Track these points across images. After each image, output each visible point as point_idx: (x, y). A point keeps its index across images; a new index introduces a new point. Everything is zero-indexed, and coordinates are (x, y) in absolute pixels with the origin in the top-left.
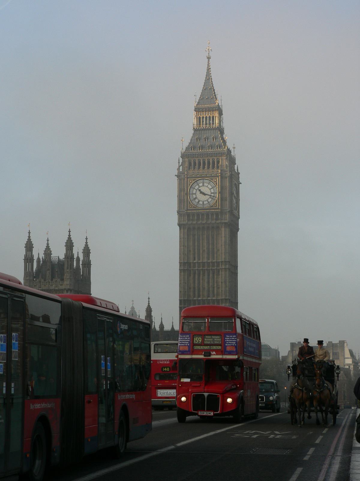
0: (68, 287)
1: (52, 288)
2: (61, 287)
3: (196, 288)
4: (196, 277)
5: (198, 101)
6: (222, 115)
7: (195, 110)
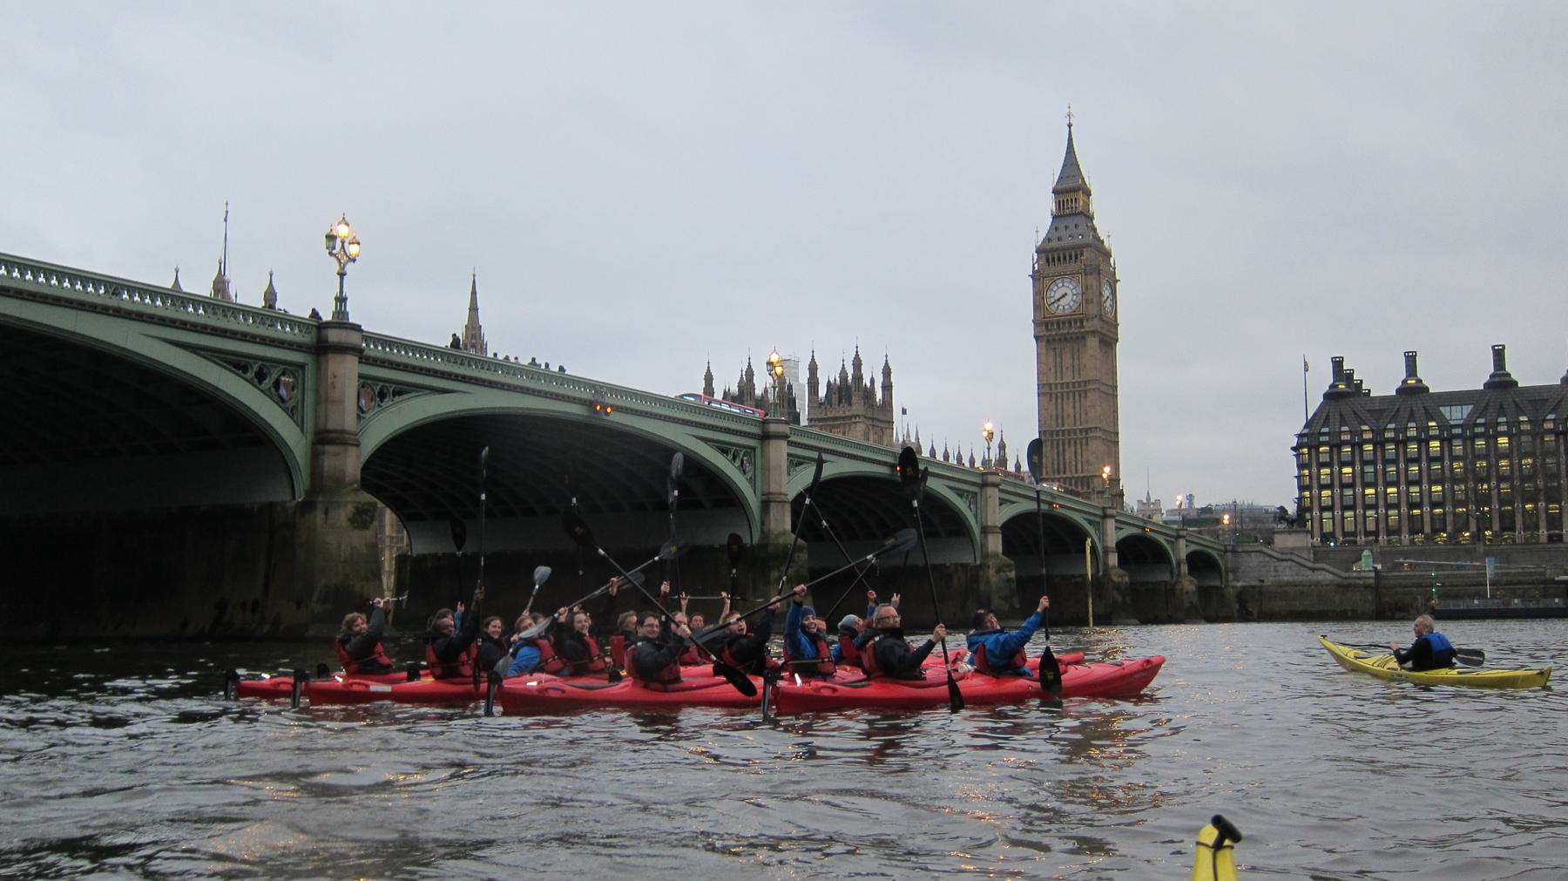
0: (855, 413)
1: (837, 415)
2: (848, 414)
3: (1060, 417)
4: (1059, 401)
5: (1056, 181)
6: (1090, 195)
7: (1053, 192)
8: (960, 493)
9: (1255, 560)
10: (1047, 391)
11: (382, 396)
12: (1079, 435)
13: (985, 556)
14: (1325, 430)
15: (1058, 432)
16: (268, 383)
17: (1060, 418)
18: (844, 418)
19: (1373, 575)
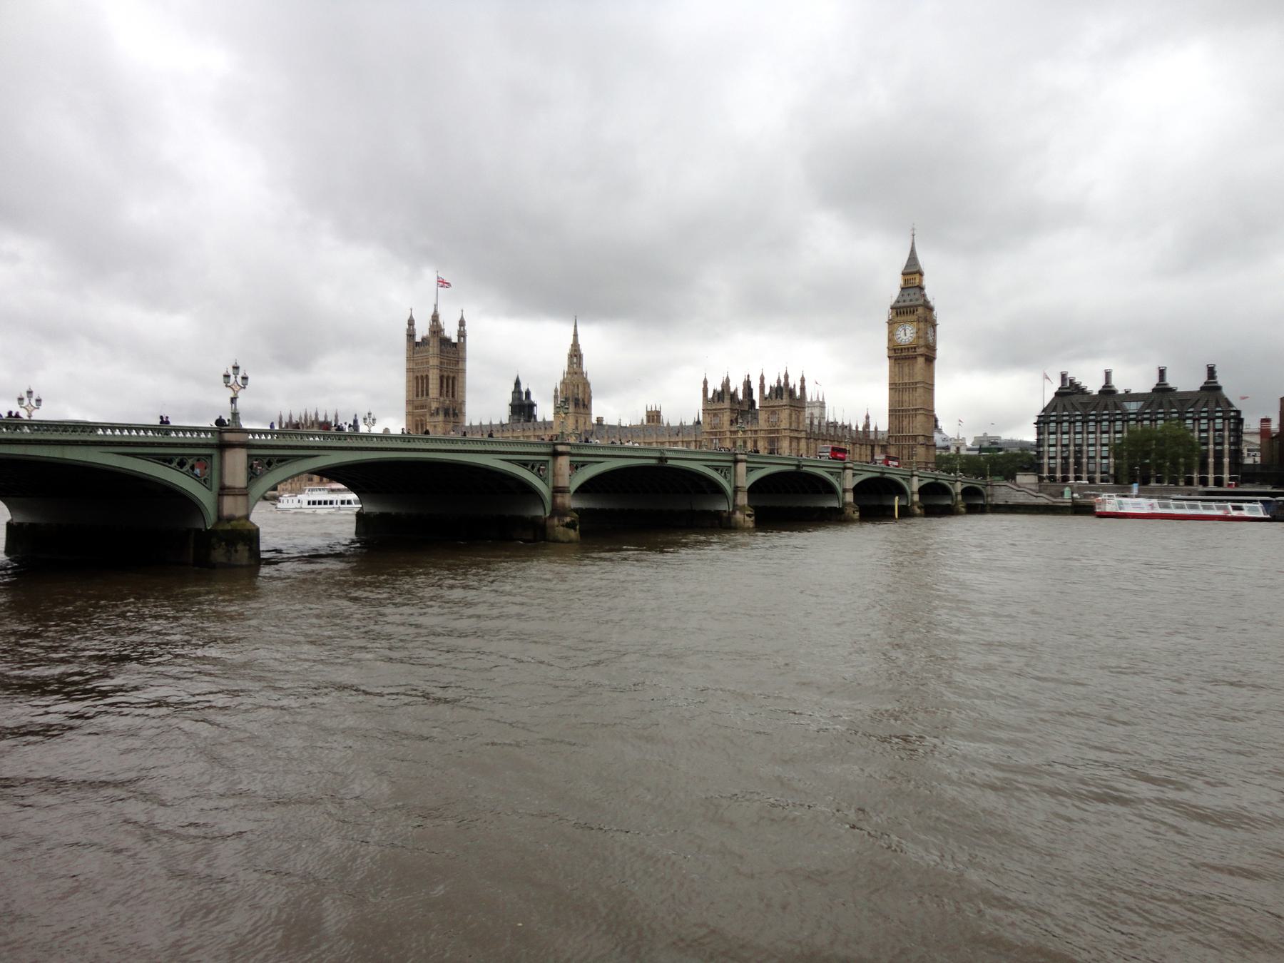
8: (832, 474)
9: (1003, 490)
10: (894, 387)
11: (577, 468)
12: (911, 412)
13: (845, 504)
14: (1053, 414)
15: (899, 410)
16: (536, 469)
17: (901, 402)
18: (778, 406)
19: (1071, 501)
